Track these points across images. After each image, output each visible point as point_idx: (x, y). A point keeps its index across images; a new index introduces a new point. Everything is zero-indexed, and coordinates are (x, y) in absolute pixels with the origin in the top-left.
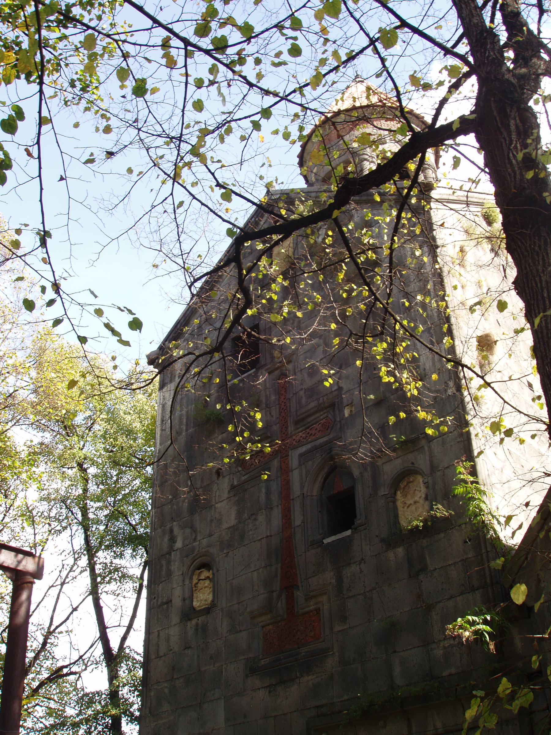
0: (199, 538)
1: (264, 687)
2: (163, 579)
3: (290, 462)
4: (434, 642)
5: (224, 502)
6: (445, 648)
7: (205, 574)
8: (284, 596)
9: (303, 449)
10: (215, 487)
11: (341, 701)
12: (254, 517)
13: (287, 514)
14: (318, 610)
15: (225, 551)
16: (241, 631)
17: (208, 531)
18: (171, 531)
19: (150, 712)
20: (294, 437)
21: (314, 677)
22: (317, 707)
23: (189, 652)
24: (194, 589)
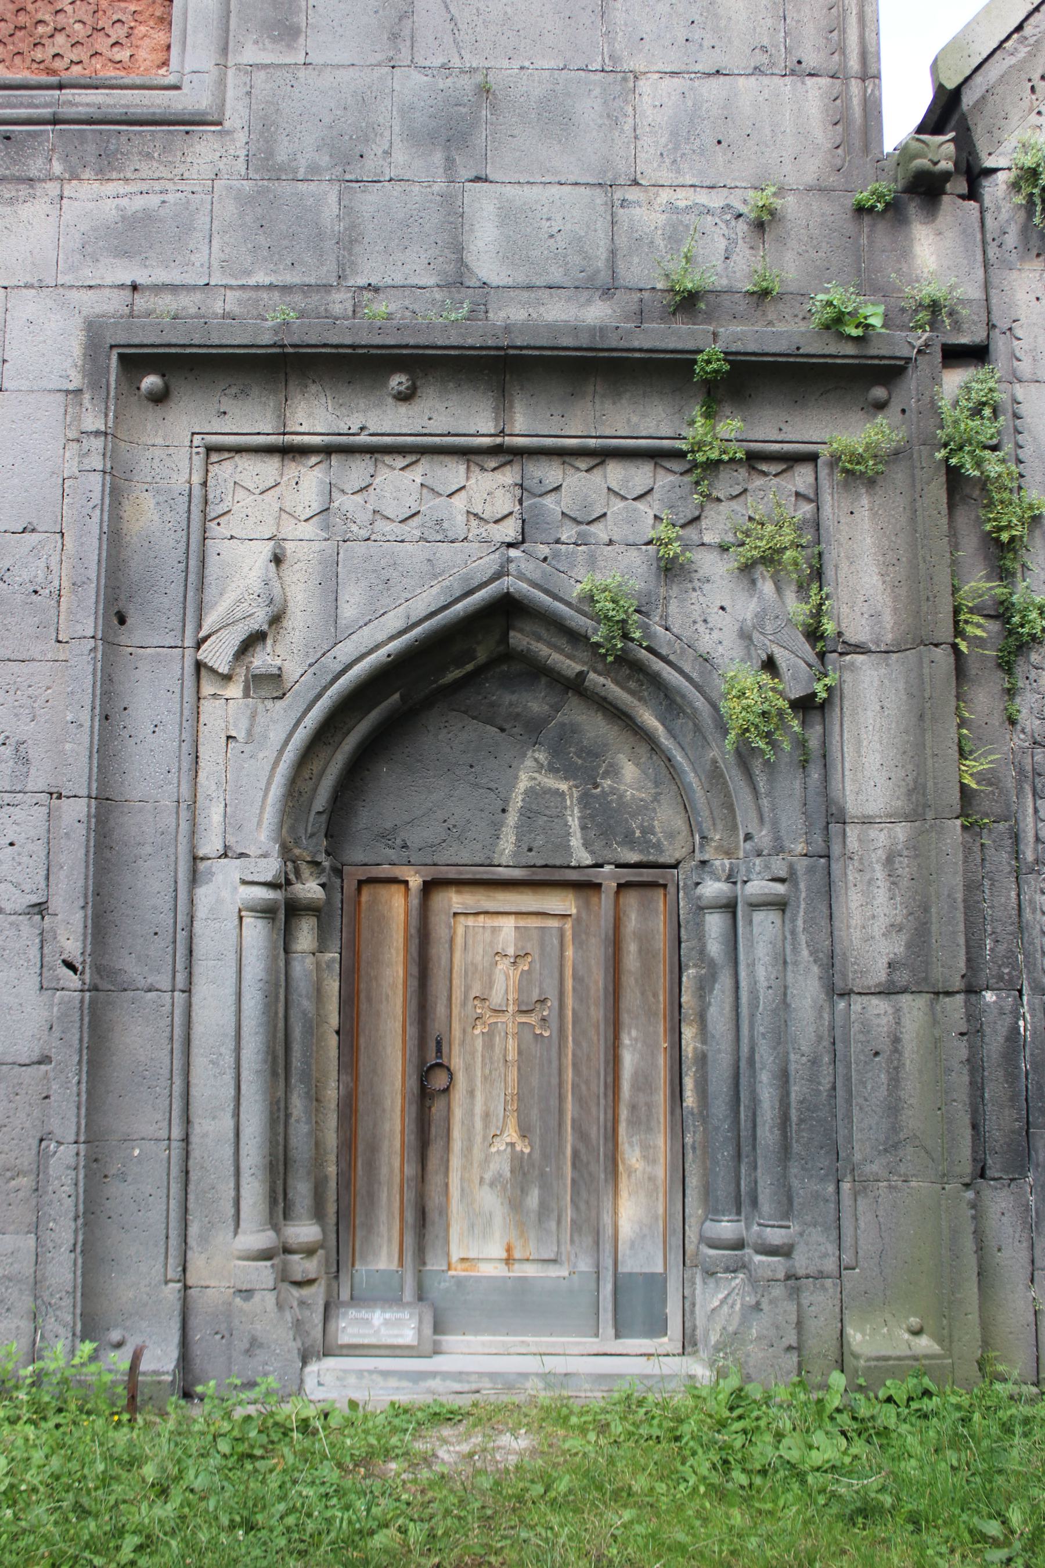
4: (636, 183)
6: (671, 208)
11: (242, 287)
21: (129, 188)
22: (135, 287)
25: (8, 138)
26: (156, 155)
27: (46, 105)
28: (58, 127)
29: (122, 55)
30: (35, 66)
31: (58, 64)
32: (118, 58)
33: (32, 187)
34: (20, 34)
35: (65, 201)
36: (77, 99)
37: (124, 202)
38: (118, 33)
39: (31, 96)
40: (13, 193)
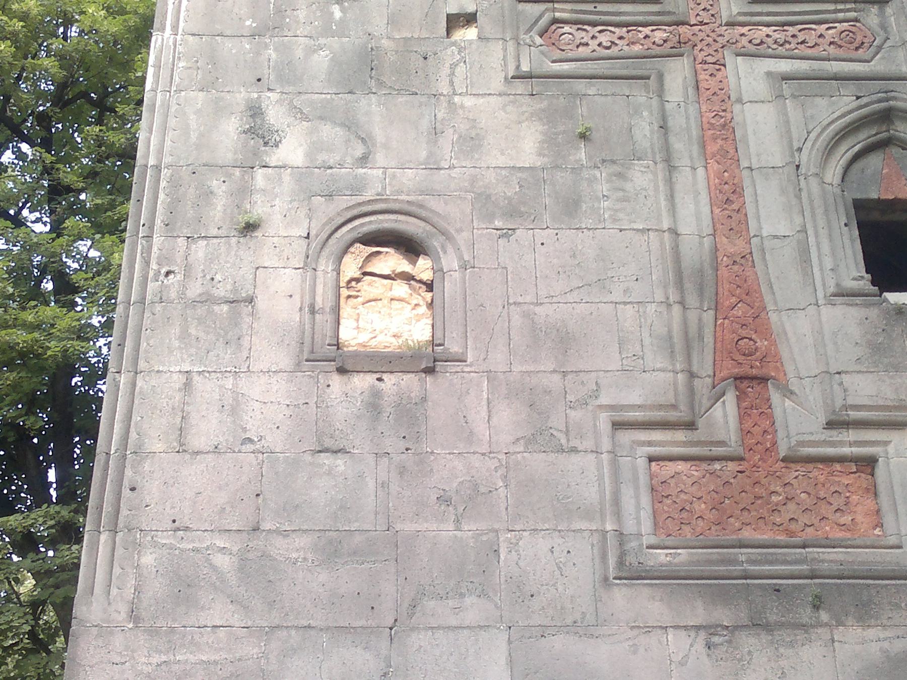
0: (380, 158)
1: (686, 628)
2: (215, 232)
3: (732, 80)
5: (492, 99)
7: (391, 261)
8: (730, 398)
9: (785, 66)
10: (450, 54)
12: (616, 168)
13: (729, 199)
14: (868, 464)
15: (498, 223)
16: (574, 450)
17: (424, 154)
18: (255, 111)
19: (134, 615)
20: (744, 30)
21: (888, 634)
23: (340, 463)
24: (344, 292)
25: (778, 591)
26: (903, 605)
27: (796, 562)
28: (817, 581)
29: (846, 519)
30: (777, 528)
31: (793, 526)
32: (842, 520)
33: (806, 632)
34: (759, 502)
35: (836, 644)
36: (822, 556)
37: (886, 645)
38: (837, 502)
39: (785, 554)
40: (792, 638)
